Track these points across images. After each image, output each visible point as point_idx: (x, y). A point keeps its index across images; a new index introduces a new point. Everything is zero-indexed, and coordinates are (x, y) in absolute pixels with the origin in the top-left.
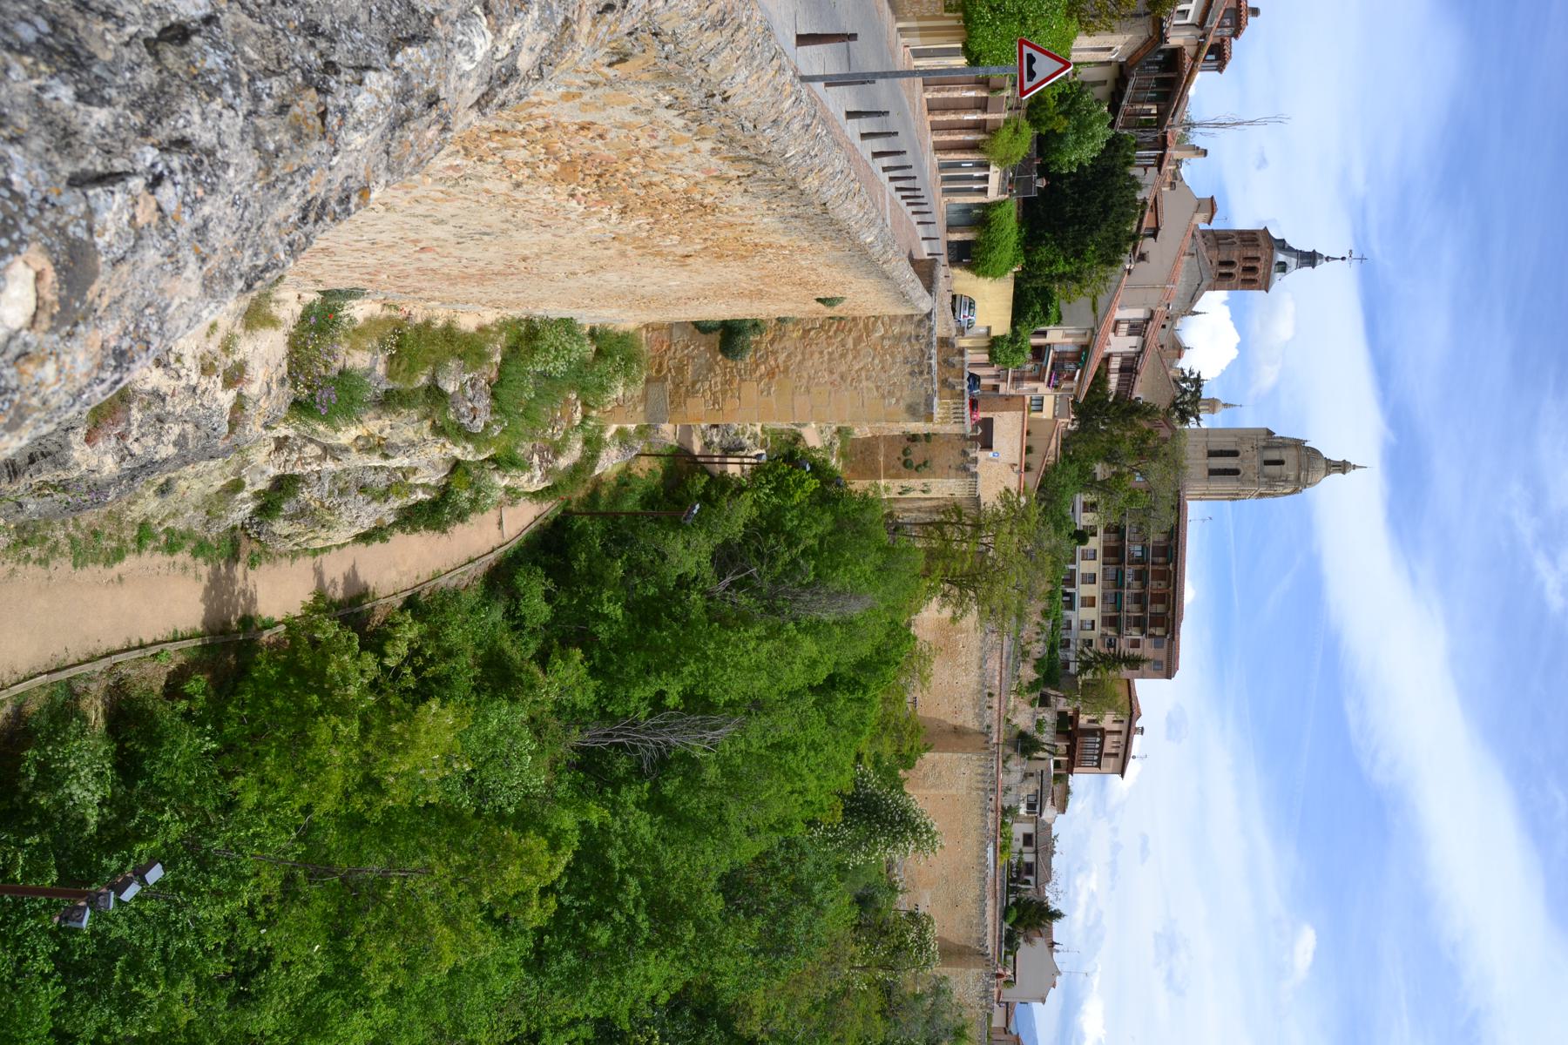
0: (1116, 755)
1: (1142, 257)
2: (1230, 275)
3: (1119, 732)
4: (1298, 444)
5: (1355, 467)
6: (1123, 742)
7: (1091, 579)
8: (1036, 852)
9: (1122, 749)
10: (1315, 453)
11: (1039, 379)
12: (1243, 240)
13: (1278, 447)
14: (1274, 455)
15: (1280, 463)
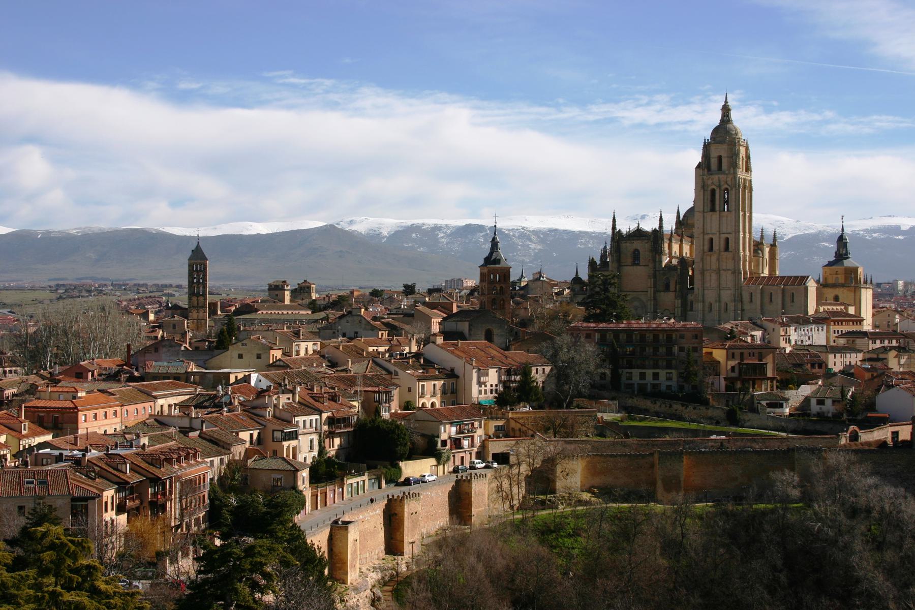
0: (760, 354)
1: (452, 370)
2: (501, 288)
3: (742, 354)
4: (707, 147)
5: (726, 102)
6: (750, 351)
7: (643, 376)
8: (827, 398)
9: (754, 351)
10: (716, 131)
11: (472, 437)
12: (483, 281)
13: (710, 158)
14: (714, 162)
15: (720, 158)
